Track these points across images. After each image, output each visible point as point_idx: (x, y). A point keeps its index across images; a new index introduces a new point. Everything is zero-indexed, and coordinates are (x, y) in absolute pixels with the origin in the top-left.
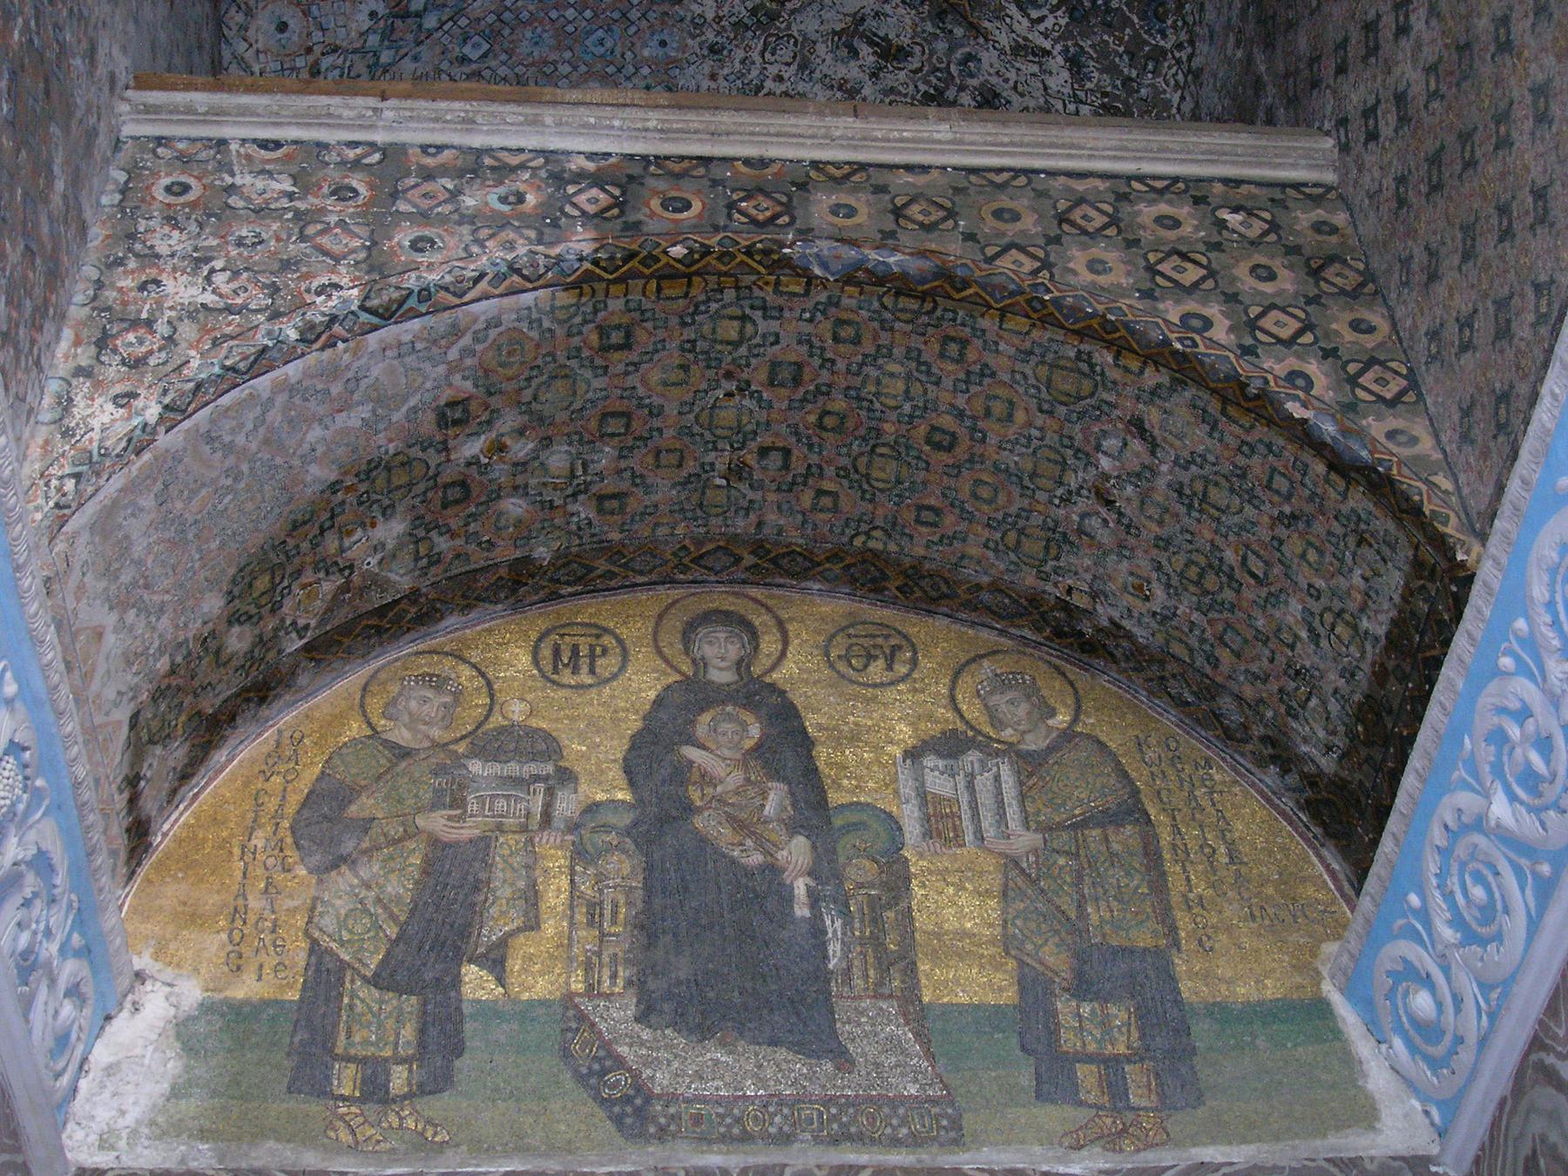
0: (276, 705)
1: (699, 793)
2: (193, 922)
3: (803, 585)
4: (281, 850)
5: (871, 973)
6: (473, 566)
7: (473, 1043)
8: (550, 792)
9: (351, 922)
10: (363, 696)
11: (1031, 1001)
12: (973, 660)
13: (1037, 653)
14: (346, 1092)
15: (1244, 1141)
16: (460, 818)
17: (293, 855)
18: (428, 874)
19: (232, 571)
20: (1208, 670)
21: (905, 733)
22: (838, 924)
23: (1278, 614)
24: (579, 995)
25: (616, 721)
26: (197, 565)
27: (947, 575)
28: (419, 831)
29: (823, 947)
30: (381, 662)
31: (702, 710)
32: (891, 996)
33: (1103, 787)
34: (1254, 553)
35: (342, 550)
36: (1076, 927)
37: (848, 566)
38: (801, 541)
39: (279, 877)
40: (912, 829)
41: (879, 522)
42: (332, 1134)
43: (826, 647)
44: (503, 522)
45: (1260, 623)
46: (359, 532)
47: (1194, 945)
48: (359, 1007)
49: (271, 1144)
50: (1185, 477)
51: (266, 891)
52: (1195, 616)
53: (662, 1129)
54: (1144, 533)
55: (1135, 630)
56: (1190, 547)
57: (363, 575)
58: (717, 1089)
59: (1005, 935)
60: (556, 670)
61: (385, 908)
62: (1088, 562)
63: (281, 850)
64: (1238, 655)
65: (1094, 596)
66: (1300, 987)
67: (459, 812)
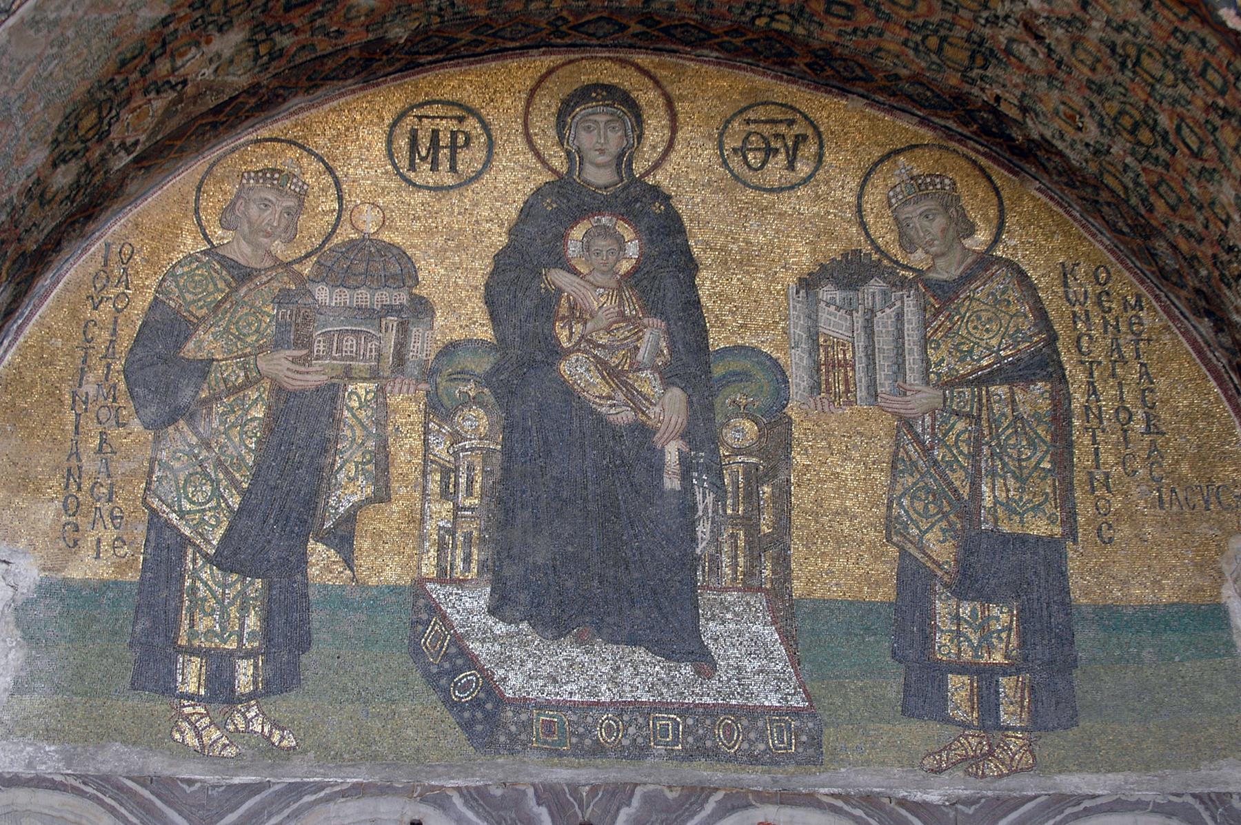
0: (103, 217)
1: (566, 332)
2: (26, 487)
3: (698, 52)
4: (115, 399)
5: (741, 560)
6: (318, 54)
7: (321, 635)
8: (403, 328)
9: (191, 490)
10: (197, 199)
11: (908, 599)
12: (888, 156)
13: (961, 149)
14: (192, 688)
15: (1113, 769)
16: (305, 361)
17: (127, 408)
18: (272, 430)
19: (55, 124)
20: (1143, 211)
21: (802, 257)
22: (710, 498)
23: (1211, 189)
24: (431, 580)
25: (478, 236)
26: (21, 132)
27: (861, 61)
28: (262, 376)
29: (690, 528)
30: (217, 152)
31: (575, 221)
32: (760, 589)
33: (1018, 331)
34: (1188, 126)
35: (174, 70)
36: (968, 509)
37: (751, 41)
38: (695, 16)
39: (114, 432)
40: (799, 381)
41: (782, 8)
42: (177, 736)
43: (721, 135)
44: (353, 13)
45: (1195, 190)
46: (194, 50)
47: (1093, 535)
48: (202, 592)
49: (117, 746)
50: (1119, 39)
51: (100, 450)
52: (1128, 160)
53: (513, 738)
54: (1075, 73)
55: (1068, 152)
56: (1122, 99)
57: (197, 86)
58: (571, 693)
59: (888, 517)
60: (412, 167)
61: (227, 473)
62: (1016, 80)
63: (115, 399)
64: (1173, 209)
65: (1024, 110)
66: (1199, 589)
67: (304, 352)
